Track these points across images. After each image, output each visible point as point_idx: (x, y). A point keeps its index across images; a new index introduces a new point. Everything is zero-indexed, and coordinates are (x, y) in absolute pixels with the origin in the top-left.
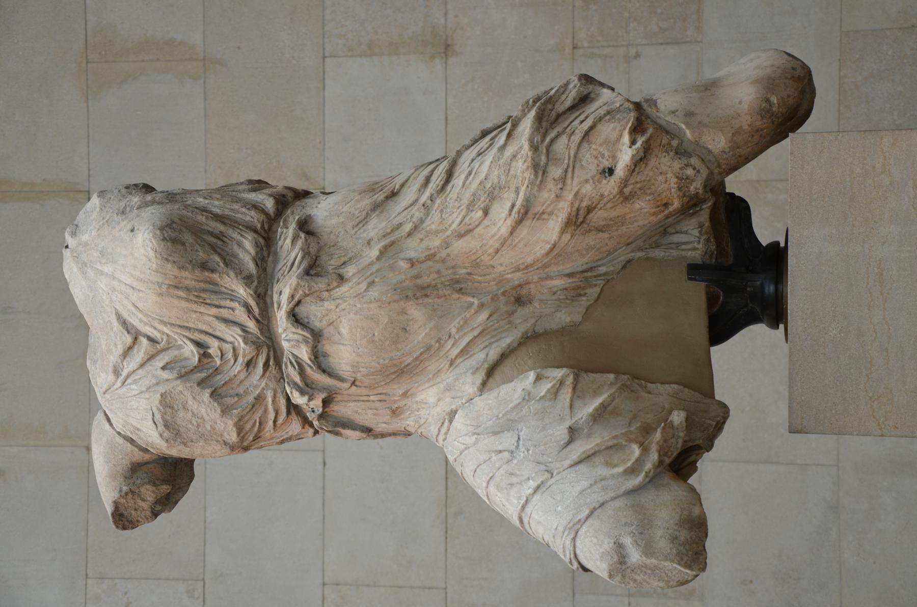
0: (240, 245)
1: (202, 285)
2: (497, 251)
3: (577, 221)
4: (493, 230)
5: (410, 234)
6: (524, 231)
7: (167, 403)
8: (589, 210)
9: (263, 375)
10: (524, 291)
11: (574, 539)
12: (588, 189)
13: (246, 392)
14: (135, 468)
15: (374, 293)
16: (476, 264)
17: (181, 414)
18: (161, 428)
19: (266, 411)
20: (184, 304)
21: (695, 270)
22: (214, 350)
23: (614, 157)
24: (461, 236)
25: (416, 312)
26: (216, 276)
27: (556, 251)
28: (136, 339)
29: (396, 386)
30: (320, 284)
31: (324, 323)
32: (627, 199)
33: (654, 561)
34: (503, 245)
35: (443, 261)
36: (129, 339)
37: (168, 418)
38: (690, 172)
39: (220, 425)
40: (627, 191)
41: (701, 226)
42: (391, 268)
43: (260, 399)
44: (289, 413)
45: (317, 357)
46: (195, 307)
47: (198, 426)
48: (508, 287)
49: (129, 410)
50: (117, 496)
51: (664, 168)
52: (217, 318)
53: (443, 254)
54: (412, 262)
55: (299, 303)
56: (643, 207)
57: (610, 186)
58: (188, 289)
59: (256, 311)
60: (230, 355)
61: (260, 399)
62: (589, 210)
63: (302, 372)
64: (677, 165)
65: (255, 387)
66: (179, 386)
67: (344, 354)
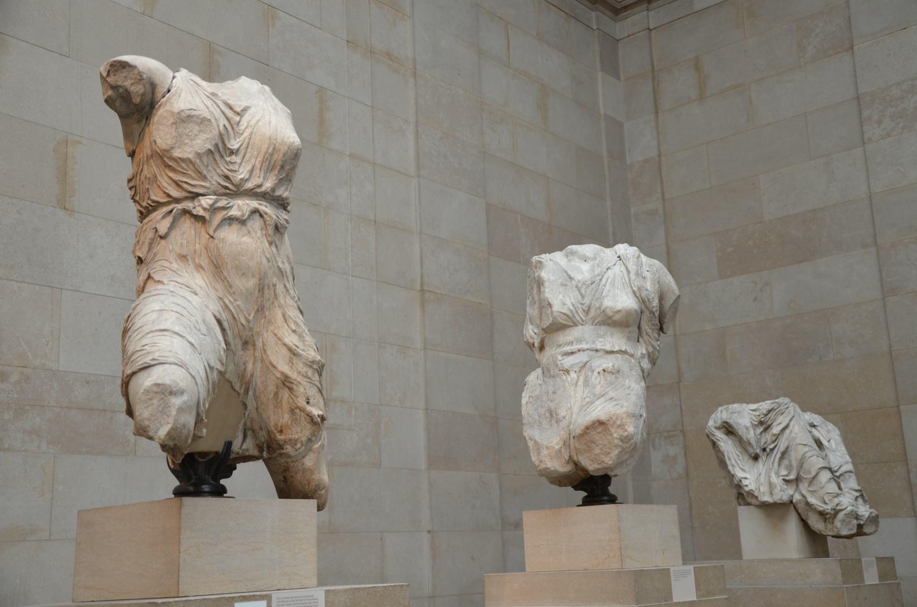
0: (286, 189)
1: (272, 163)
2: (275, 335)
3: (286, 382)
4: (286, 334)
5: (285, 286)
6: (284, 351)
7: (203, 122)
8: (291, 389)
9: (219, 184)
10: (250, 347)
11: (176, 364)
12: (302, 390)
13: (209, 171)
14: (153, 86)
15: (264, 261)
16: (270, 322)
17: (197, 128)
18: (188, 112)
19: (194, 179)
20: (264, 150)
21: (229, 445)
22: (234, 158)
23: (313, 405)
24: (284, 316)
25: (252, 283)
26: (276, 172)
27: (271, 368)
28: (238, 114)
29: (206, 261)
30: (271, 231)
31: (250, 229)
32: (292, 411)
33: (174, 413)
34: (279, 339)
35: (273, 303)
36: (239, 110)
37: (194, 119)
38: (299, 445)
39: (188, 149)
40: (298, 411)
41: (247, 450)
42: (274, 273)
43: (204, 178)
44: (190, 192)
45: (231, 220)
46: (262, 155)
47: (187, 135)
48: (255, 338)
49: (186, 92)
50: (141, 70)
51: (304, 432)
52: (254, 166)
53: (276, 304)
54: (274, 286)
55: (261, 216)
56: (286, 418)
57: (301, 402)
58: (272, 155)
59: (259, 190)
60: (231, 167)
61: (204, 178)
62: (291, 389)
63: (224, 208)
64: (304, 439)
65: (212, 177)
66: (215, 132)
67: (231, 236)
